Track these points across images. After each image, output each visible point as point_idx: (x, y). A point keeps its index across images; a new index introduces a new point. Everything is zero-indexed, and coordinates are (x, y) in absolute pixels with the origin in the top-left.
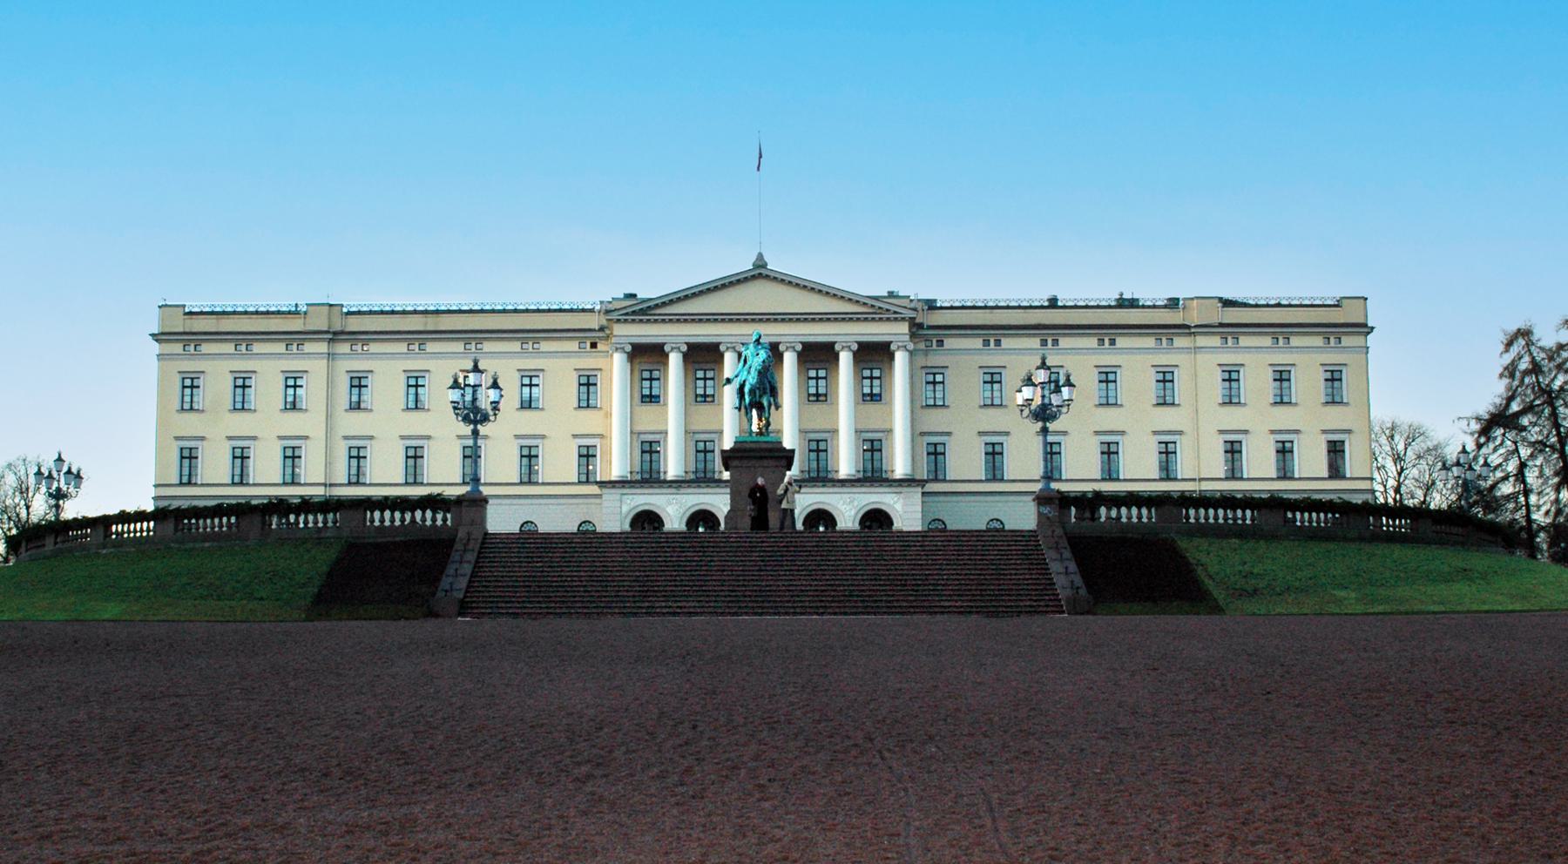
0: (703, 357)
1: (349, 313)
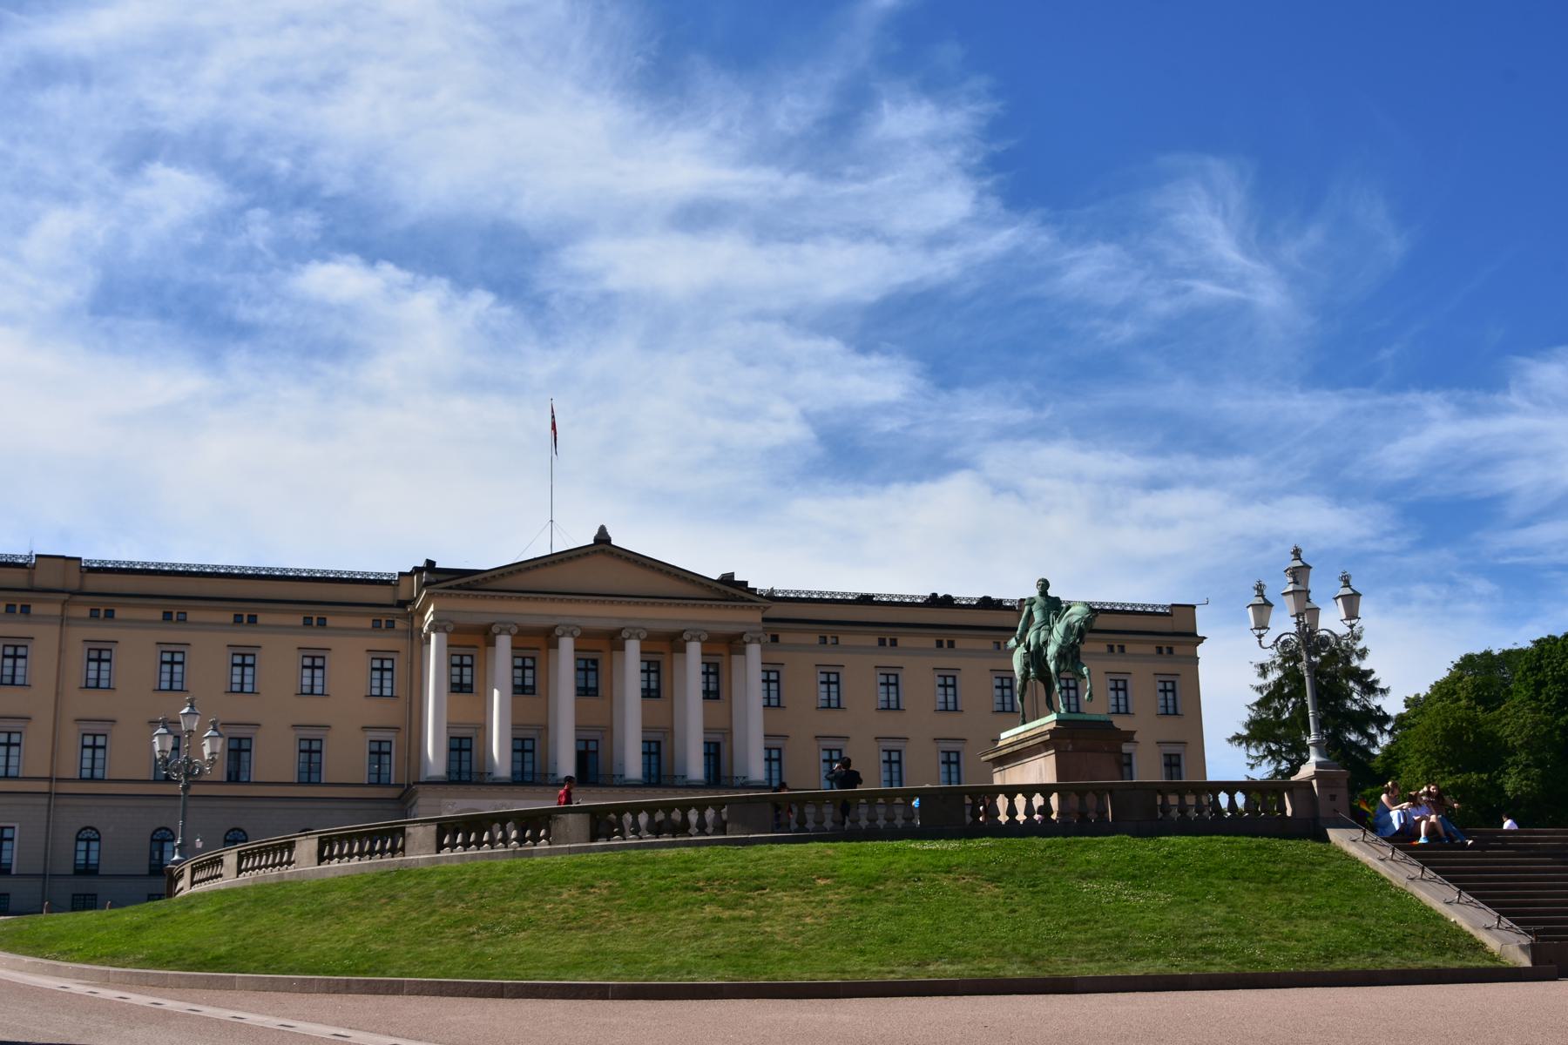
0: (535, 645)
1: (91, 570)
